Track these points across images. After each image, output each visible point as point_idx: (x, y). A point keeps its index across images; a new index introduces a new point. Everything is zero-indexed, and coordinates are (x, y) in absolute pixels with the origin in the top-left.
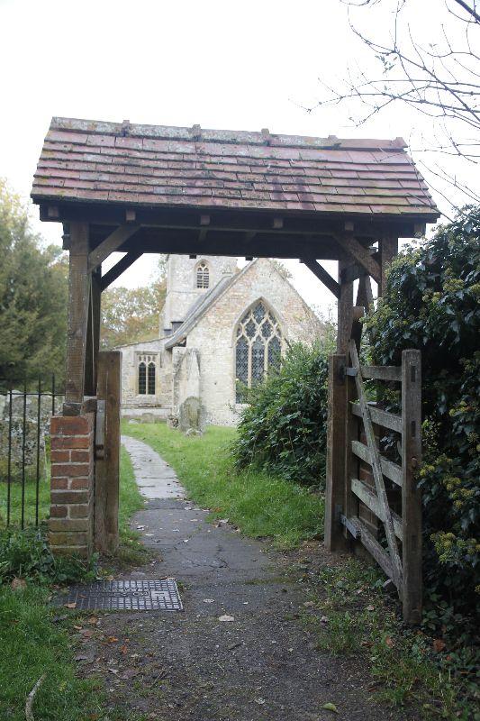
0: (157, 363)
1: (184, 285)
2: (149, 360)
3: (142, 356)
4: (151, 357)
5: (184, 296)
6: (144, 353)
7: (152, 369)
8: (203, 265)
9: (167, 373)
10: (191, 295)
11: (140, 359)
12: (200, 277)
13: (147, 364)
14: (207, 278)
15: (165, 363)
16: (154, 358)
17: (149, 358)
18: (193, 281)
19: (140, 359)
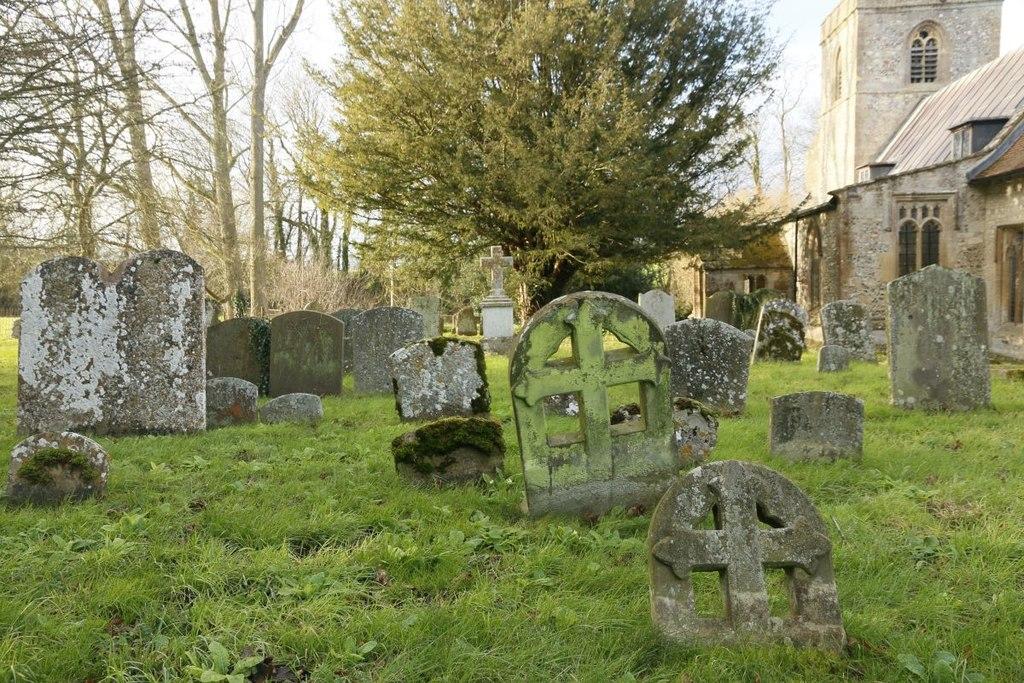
0: (944, 220)
1: (885, 79)
2: (924, 215)
3: (908, 207)
4: (931, 207)
5: (884, 101)
6: (916, 197)
7: (932, 232)
8: (924, 35)
9: (972, 242)
10: (899, 98)
11: (902, 213)
12: (916, 59)
13: (920, 223)
14: (932, 62)
15: (966, 220)
16: (936, 209)
17: (925, 211)
18: (903, 68)
19: (902, 213)
